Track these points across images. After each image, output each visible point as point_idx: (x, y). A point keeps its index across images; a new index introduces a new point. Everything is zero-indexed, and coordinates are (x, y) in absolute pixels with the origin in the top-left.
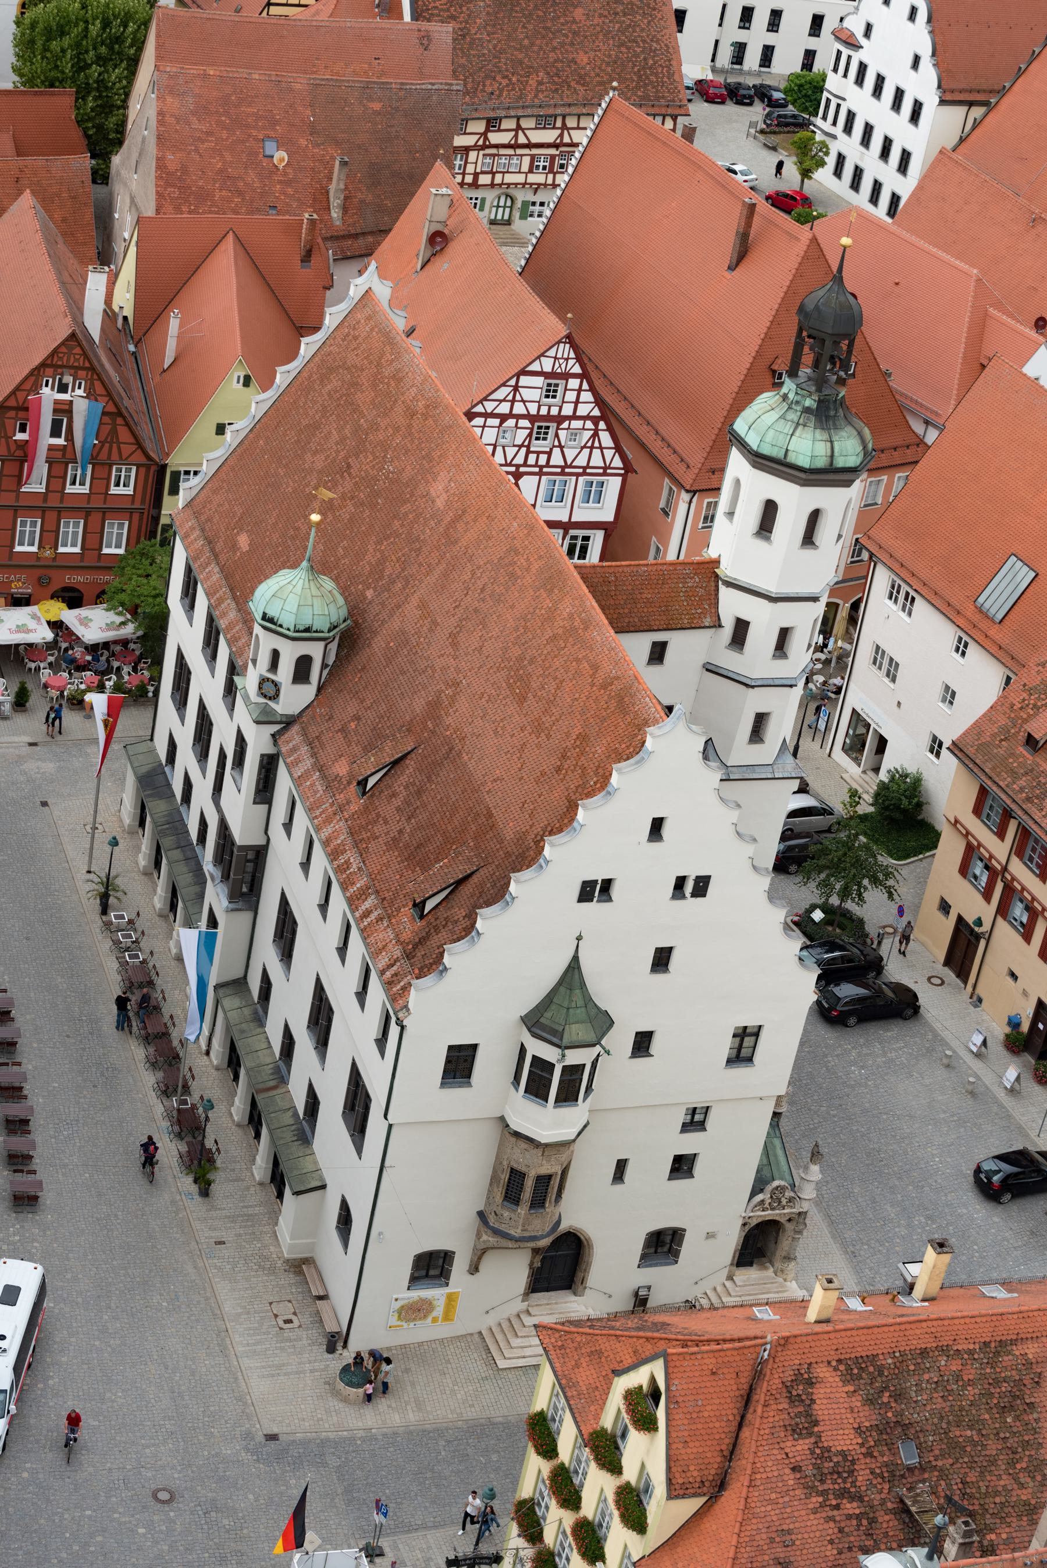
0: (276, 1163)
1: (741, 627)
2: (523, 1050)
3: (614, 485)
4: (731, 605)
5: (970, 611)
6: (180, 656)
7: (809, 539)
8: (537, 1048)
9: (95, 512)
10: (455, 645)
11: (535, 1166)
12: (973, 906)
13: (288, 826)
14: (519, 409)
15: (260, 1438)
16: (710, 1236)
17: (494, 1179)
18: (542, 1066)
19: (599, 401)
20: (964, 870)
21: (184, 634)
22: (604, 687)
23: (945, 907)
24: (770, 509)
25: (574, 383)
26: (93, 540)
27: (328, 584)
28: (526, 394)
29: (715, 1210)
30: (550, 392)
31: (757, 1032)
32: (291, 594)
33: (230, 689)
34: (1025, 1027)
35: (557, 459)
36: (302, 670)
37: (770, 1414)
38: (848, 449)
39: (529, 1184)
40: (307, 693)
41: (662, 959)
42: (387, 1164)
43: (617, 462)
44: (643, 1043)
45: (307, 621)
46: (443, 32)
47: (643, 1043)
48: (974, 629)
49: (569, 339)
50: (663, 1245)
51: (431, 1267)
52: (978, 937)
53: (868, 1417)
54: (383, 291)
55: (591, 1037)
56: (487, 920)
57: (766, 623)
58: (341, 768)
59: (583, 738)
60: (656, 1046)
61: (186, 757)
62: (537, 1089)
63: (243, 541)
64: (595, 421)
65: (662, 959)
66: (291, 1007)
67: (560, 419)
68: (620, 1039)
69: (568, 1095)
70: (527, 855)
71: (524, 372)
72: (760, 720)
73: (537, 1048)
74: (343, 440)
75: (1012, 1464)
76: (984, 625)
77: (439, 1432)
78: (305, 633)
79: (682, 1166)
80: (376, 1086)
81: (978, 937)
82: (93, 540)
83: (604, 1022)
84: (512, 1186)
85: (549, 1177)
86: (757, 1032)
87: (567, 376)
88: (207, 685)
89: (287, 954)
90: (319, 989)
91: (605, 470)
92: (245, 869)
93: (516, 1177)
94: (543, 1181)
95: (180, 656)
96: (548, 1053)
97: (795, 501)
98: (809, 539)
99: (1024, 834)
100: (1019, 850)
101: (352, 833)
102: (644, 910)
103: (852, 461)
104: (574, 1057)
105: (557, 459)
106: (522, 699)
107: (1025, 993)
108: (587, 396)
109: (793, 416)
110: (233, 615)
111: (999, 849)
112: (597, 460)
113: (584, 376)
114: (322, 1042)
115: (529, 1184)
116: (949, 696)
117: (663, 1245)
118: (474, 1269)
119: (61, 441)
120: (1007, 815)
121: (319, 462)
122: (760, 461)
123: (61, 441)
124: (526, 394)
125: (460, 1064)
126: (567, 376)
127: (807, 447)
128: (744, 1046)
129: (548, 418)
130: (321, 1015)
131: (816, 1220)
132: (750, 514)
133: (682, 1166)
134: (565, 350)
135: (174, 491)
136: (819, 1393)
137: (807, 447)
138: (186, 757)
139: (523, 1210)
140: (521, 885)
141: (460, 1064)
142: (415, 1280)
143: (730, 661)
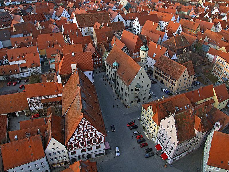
0: (120, 97)
1: (143, 61)
3: (129, 53)
4: (142, 60)
6: (107, 69)
8: (136, 88)
9: (99, 61)
12: (156, 75)
13: (117, 78)
18: (137, 89)
21: (107, 67)
23: (155, 75)
26: (99, 62)
31: (148, 85)
32: (115, 64)
33: (111, 70)
36: (116, 69)
40: (117, 69)
44: (142, 86)
46: (111, 27)
48: (153, 58)
50: (144, 98)
51: (132, 102)
53: (164, 107)
58: (120, 74)
61: (109, 74)
62: (137, 91)
66: (119, 88)
68: (141, 87)
78: (116, 66)
79: (145, 94)
80: (127, 92)
82: (99, 62)
83: (140, 86)
86: (148, 85)
88: (109, 70)
89: (119, 86)
90: (121, 87)
91: (129, 53)
92: (115, 81)
95: (107, 69)
96: (137, 88)
97: (144, 52)
98: (146, 55)
99: (159, 70)
100: (159, 71)
110: (111, 66)
111: (158, 71)
114: (122, 91)
116: (152, 62)
117: (144, 98)
118: (134, 102)
120: (158, 69)
122: (142, 51)
125: (132, 90)
127: (145, 49)
128: (148, 85)
130: (122, 89)
132: (142, 54)
133: (145, 94)
137: (145, 49)
138: (109, 74)
141: (132, 90)
143: (142, 63)
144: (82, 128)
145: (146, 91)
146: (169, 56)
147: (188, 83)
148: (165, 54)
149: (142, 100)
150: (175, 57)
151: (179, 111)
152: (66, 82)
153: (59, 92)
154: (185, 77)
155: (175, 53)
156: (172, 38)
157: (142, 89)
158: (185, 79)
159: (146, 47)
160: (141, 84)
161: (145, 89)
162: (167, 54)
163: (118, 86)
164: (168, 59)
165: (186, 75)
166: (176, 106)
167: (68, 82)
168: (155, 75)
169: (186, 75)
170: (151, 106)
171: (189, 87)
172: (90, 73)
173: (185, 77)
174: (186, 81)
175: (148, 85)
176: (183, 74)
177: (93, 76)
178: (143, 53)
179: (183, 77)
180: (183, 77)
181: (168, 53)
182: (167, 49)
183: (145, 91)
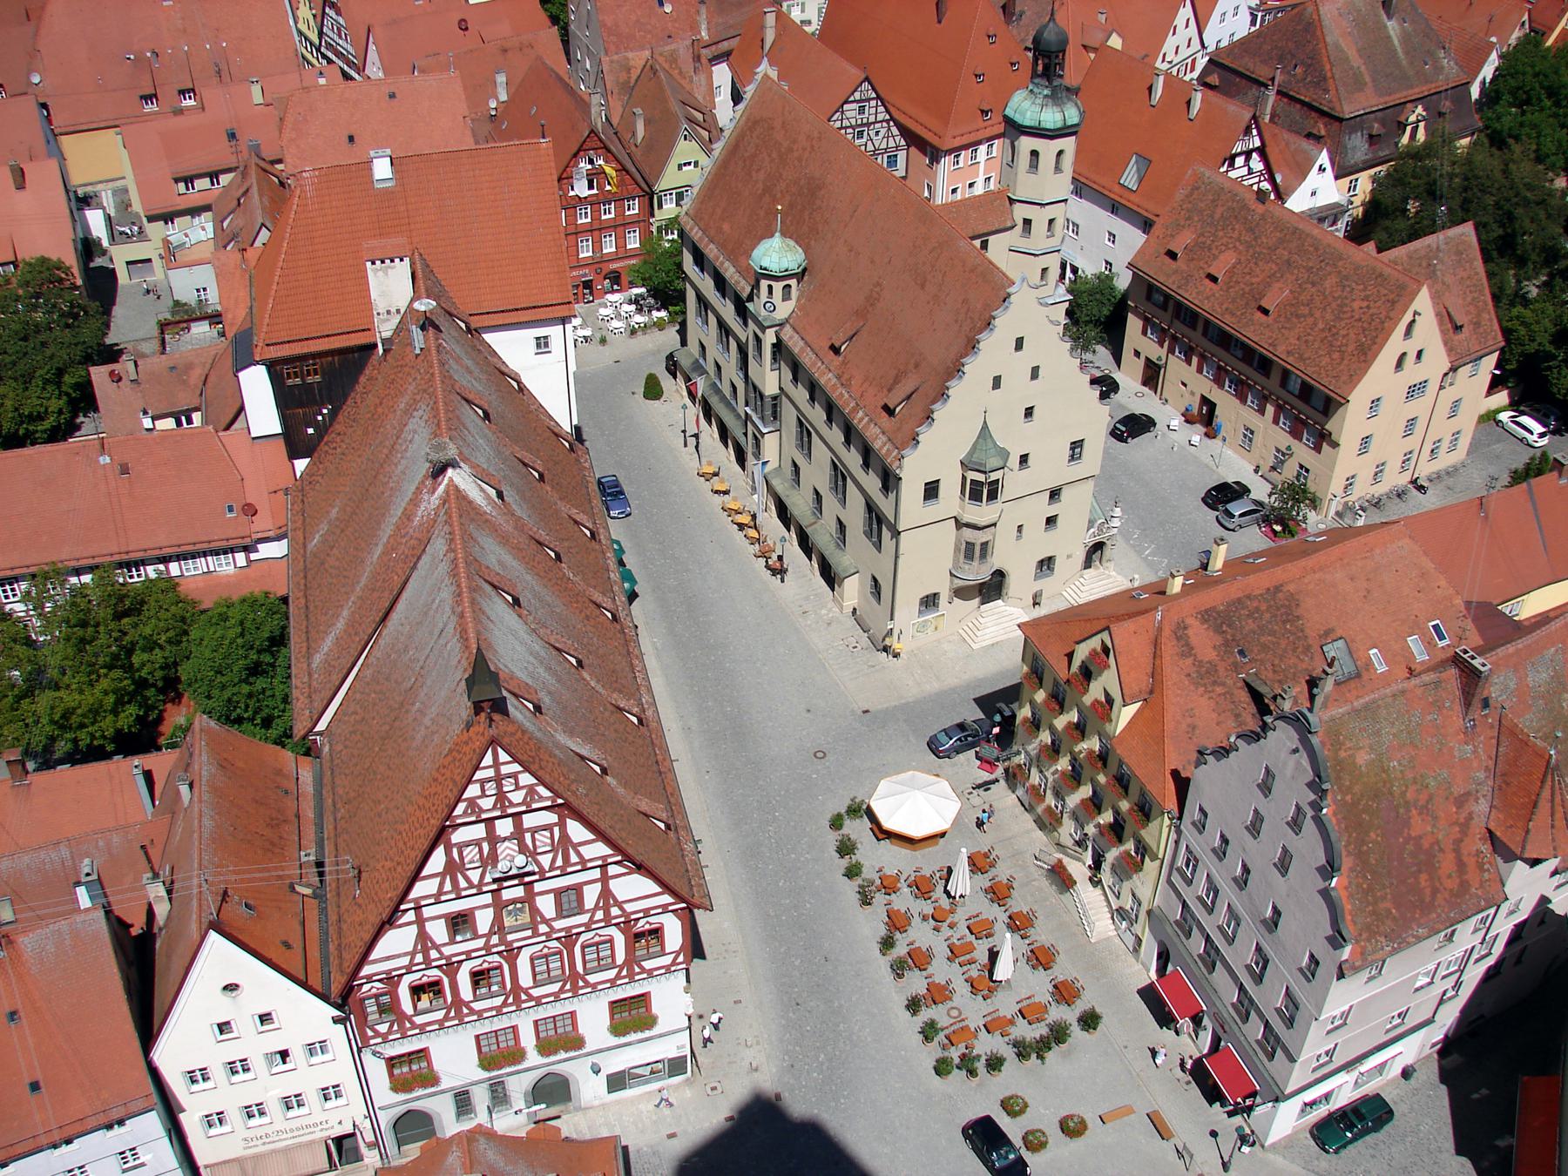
1: (1027, 222)
2: (964, 478)
5: (1117, 189)
7: (1058, 169)
8: (972, 475)
10: (872, 262)
11: (979, 538)
12: (1153, 350)
14: (846, 123)
15: (859, 712)
16: (1069, 557)
17: (957, 549)
19: (887, 111)
20: (1144, 333)
22: (972, 271)
23: (1137, 354)
24: (1035, 154)
25: (873, 103)
26: (621, 243)
27: (792, 243)
28: (848, 114)
29: (1070, 542)
30: (861, 110)
34: (1195, 411)
35: (871, 147)
37: (1169, 648)
38: (1072, 115)
39: (977, 549)
41: (1029, 412)
42: (901, 551)
43: (903, 142)
44: (1024, 459)
45: (785, 265)
47: (1024, 459)
49: (867, 79)
51: (930, 602)
52: (1159, 367)
53: (1219, 640)
54: (774, 74)
55: (1000, 464)
56: (941, 413)
57: (1040, 217)
59: (965, 301)
60: (1030, 462)
61: (714, 351)
62: (975, 495)
63: (726, 227)
64: (887, 121)
65: (1029, 412)
67: (868, 125)
68: (1014, 461)
69: (993, 496)
70: (956, 370)
71: (846, 102)
72: (1044, 270)
73: (972, 475)
74: (772, 161)
75: (1294, 650)
76: (1126, 194)
77: (954, 690)
79: (1051, 521)
81: (1159, 367)
82: (621, 243)
83: (1005, 454)
84: (969, 551)
85: (987, 543)
87: (869, 100)
93: (970, 546)
94: (985, 545)
97: (1048, 148)
98: (1058, 169)
101: (839, 377)
102: (1019, 390)
103: (1075, 120)
104: (993, 476)
105: (871, 147)
106: (923, 286)
107: (1193, 393)
108: (881, 109)
109: (1039, 101)
112: (892, 144)
113: (878, 97)
115: (977, 549)
119: (595, 191)
121: (762, 175)
123: (595, 191)
124: (848, 114)
125: (931, 491)
126: (869, 100)
127: (1051, 118)
129: (862, 125)
131: (1120, 541)
133: (1051, 521)
134: (866, 85)
135: (660, 206)
136: (1190, 632)
138: (714, 351)
139: (975, 563)
140: (956, 389)
141: (931, 491)
142: (920, 612)
143: (1023, 244)
144: (477, 843)
145: (1064, 494)
146: (1272, 180)
147: (1442, 428)
148: (1232, 158)
149: (1021, 581)
150: (1319, 189)
151: (1358, 676)
152: (322, 430)
153: (263, 523)
154: (1412, 373)
155: (1324, 154)
156: (1300, 14)
157: (1014, 482)
158: (1415, 390)
159: (1057, 96)
160: (1012, 437)
161: (1053, 485)
162: (1248, 159)
163: (801, 461)
164: (1260, 208)
165: (1419, 354)
166: (1328, 635)
167: (337, 427)
168: (1137, 354)
169: (1419, 354)
170: (1105, 636)
171: (1445, 460)
172: (542, 344)
173: (1412, 373)
174: (1420, 407)
175: (1077, 445)
176: (1395, 344)
177: (572, 367)
178: (1035, 154)
179: (1399, 364)
180: (1399, 364)
181: (1261, 151)
182: (1254, 117)
183: (1055, 494)
